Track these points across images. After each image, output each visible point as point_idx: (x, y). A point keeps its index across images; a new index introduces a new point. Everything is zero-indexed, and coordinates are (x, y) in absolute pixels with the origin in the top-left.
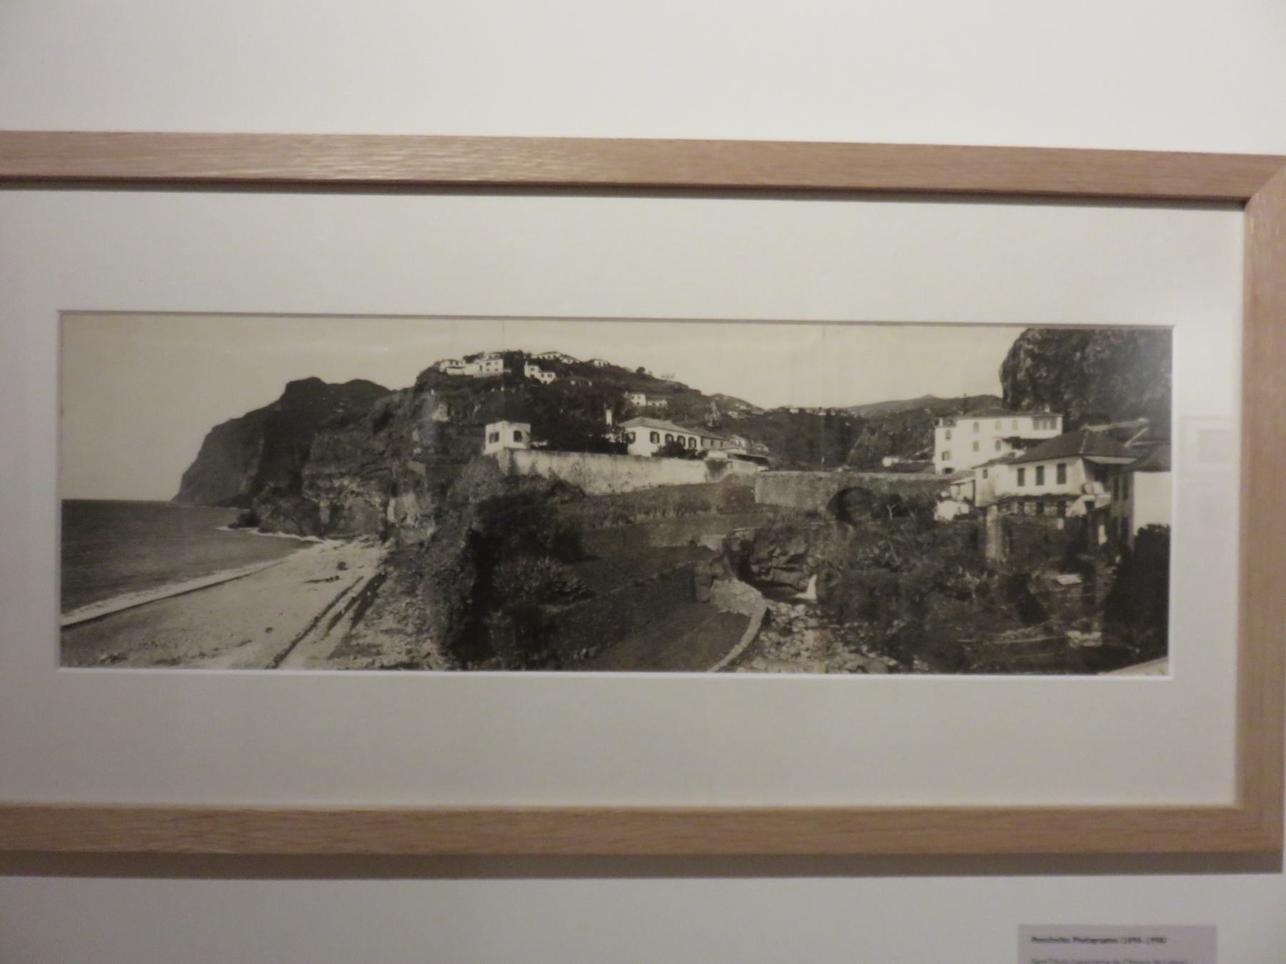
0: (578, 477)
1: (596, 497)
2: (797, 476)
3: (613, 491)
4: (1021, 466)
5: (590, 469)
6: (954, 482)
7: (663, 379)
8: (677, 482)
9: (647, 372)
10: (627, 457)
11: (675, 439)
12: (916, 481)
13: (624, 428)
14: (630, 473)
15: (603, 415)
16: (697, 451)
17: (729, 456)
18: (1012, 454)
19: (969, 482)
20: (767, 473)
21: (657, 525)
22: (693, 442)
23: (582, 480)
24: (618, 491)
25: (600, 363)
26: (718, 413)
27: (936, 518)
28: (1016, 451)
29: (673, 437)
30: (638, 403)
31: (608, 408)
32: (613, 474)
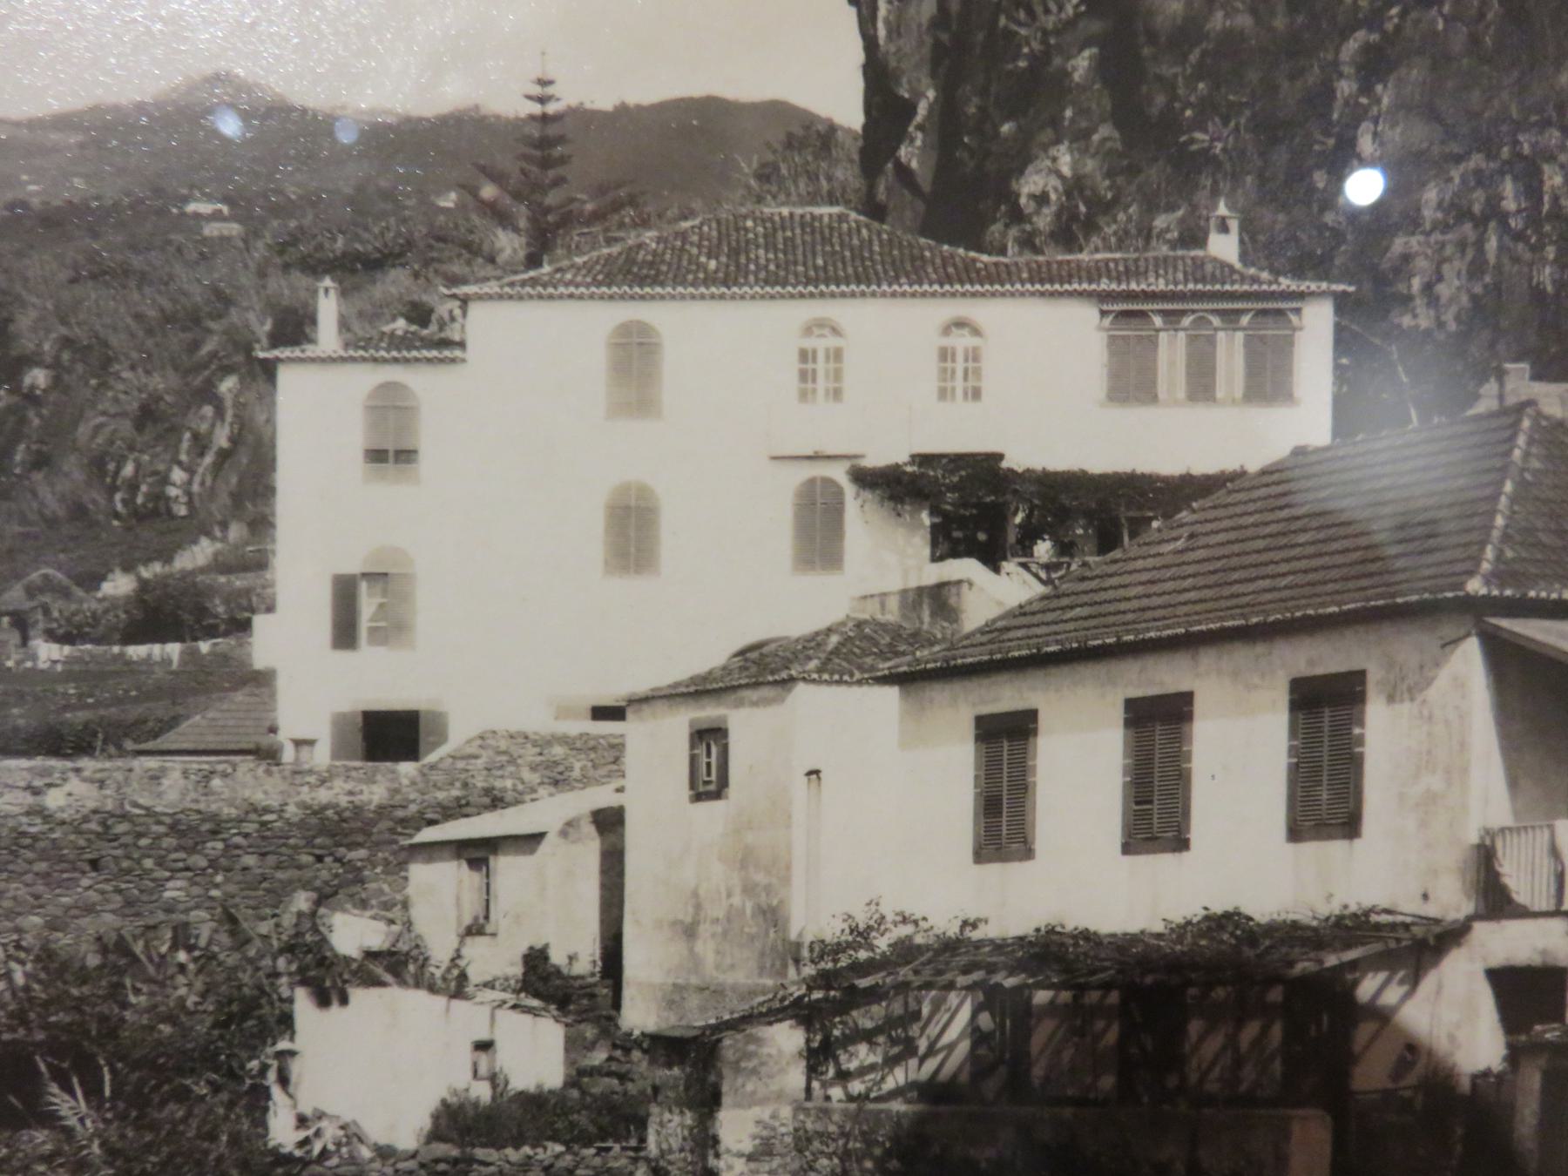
4: (1006, 696)
6: (428, 835)
12: (106, 819)
18: (939, 598)
19: (568, 829)
27: (282, 1132)
28: (967, 568)
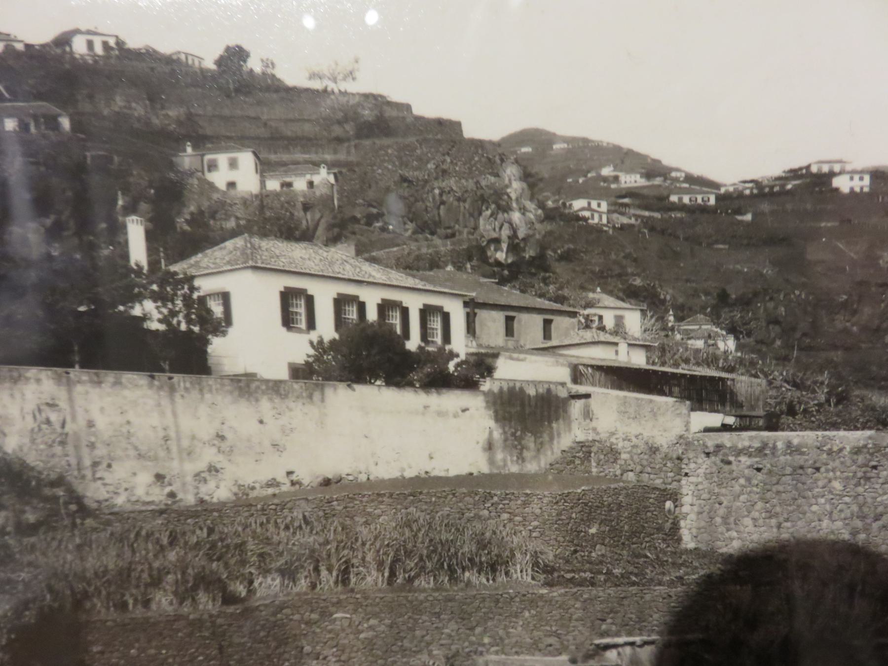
0: (58, 450)
1: (118, 515)
2: (857, 451)
3: (172, 495)
5: (91, 424)
7: (317, 85)
8: (386, 471)
9: (254, 64)
10: (209, 381)
11: (372, 315)
13: (190, 279)
14: (222, 438)
15: (117, 231)
16: (452, 355)
17: (577, 376)
20: (726, 439)
21: (325, 614)
22: (436, 324)
23: (73, 461)
24: (189, 499)
25: (90, 44)
26: (530, 206)
29: (362, 307)
30: (232, 185)
31: (131, 209)
32: (166, 439)
